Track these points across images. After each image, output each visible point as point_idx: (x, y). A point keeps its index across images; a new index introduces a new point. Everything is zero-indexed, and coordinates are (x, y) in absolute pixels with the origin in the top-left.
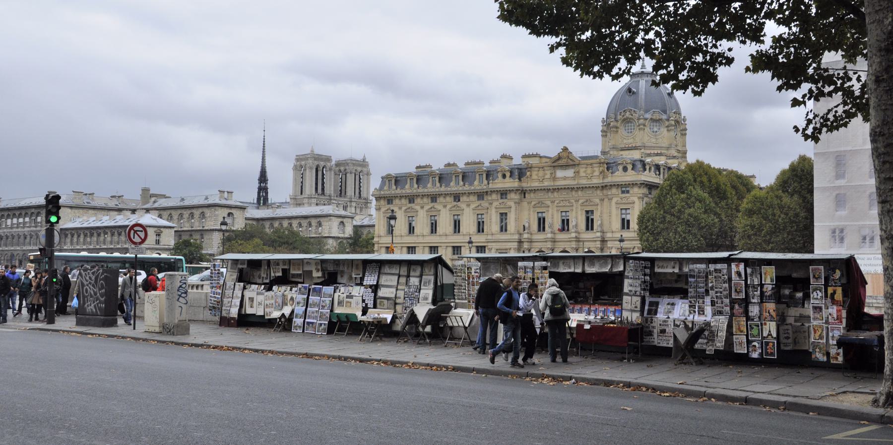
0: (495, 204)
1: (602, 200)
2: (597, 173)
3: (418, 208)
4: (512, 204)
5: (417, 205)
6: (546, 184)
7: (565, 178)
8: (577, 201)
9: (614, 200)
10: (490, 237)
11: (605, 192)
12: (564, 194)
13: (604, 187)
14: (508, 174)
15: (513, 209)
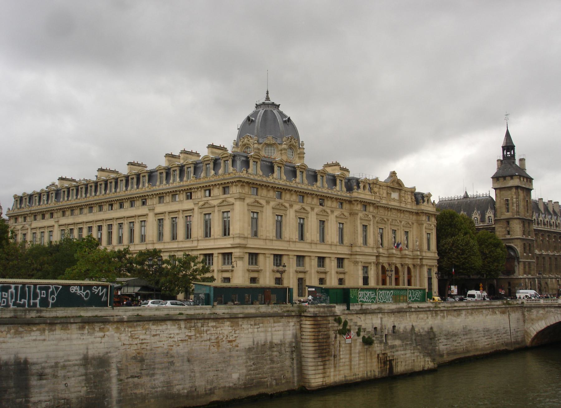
0: (361, 215)
1: (413, 224)
2: (409, 200)
3: (287, 205)
4: (370, 216)
5: (286, 201)
6: (384, 202)
7: (394, 200)
8: (401, 222)
9: (425, 225)
10: (358, 249)
11: (414, 217)
12: (392, 215)
13: (417, 214)
14: (367, 186)
15: (372, 223)
